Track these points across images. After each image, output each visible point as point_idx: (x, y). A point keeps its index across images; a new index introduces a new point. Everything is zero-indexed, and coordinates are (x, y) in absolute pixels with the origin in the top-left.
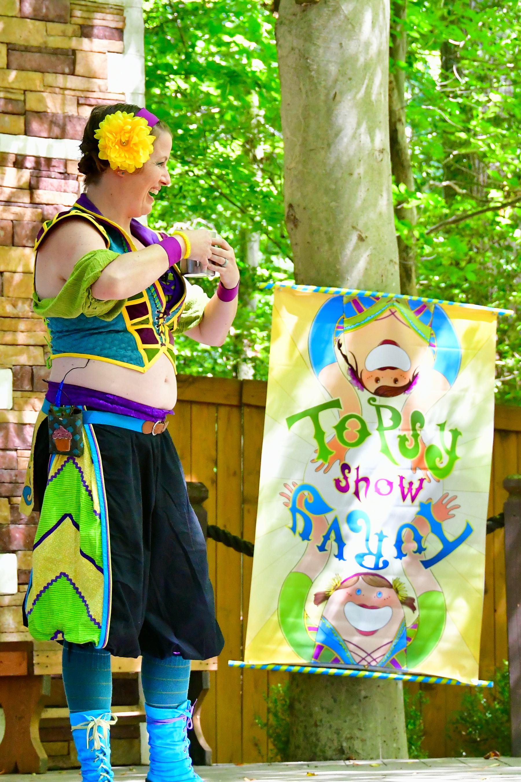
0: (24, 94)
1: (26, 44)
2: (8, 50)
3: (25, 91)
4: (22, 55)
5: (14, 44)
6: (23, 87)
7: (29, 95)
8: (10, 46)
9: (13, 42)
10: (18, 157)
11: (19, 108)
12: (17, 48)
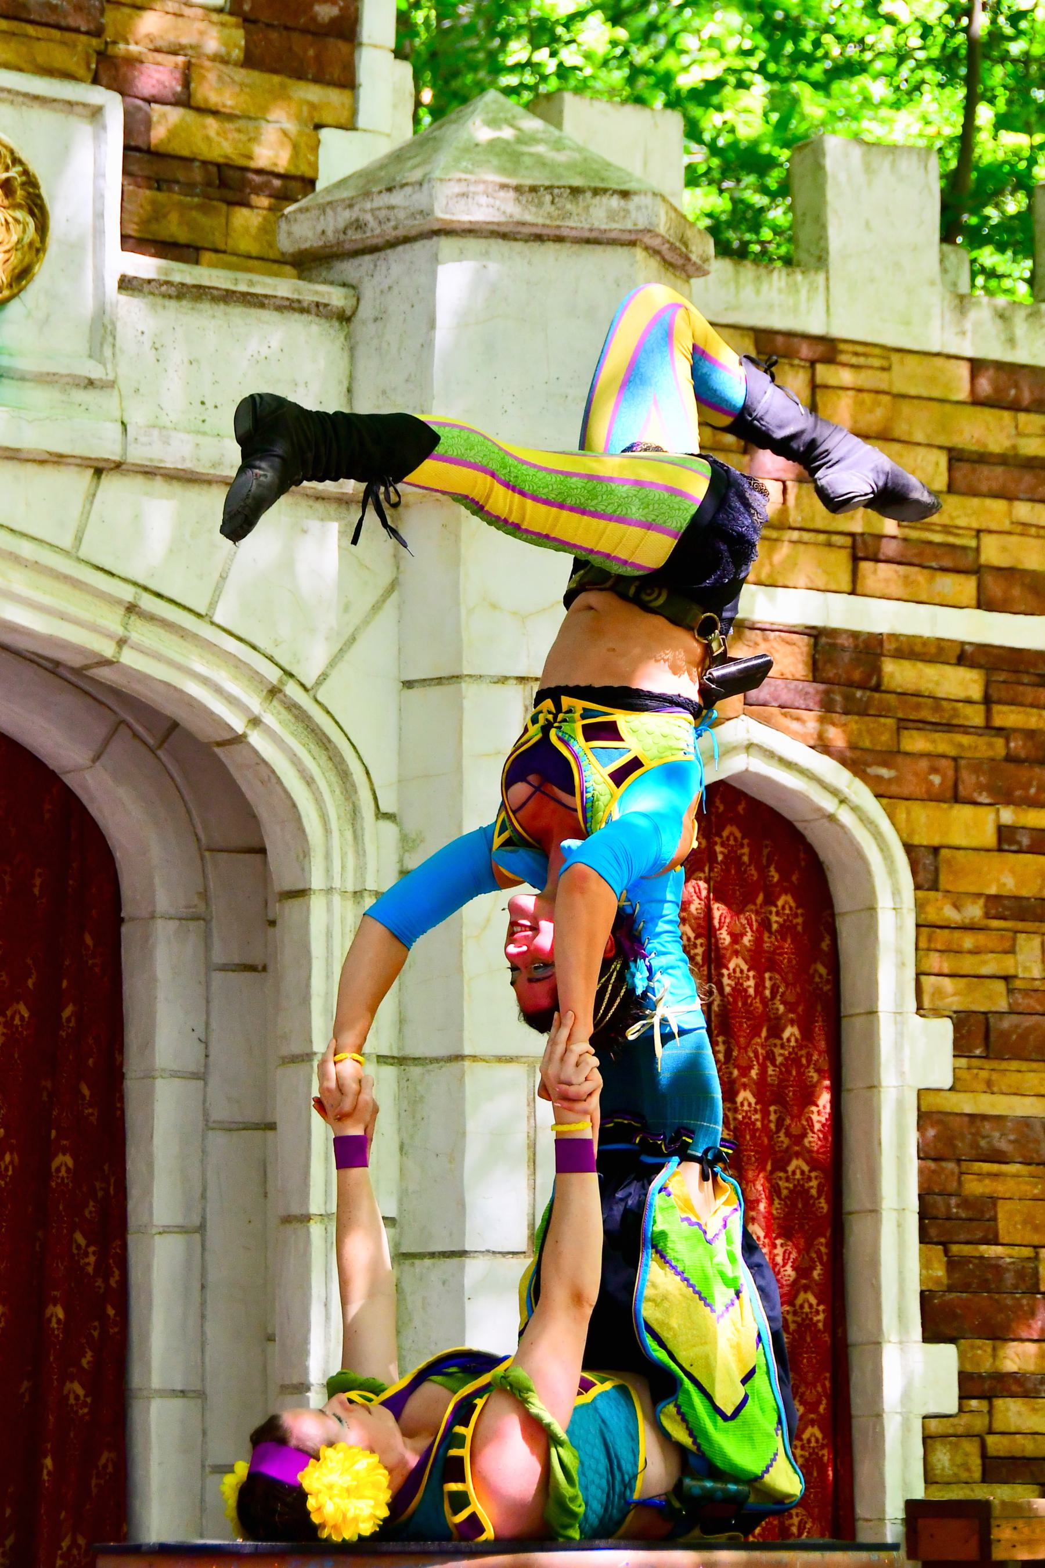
1: (982, 450)
2: (950, 461)
3: (979, 531)
4: (974, 471)
5: (962, 451)
6: (975, 525)
8: (954, 454)
9: (960, 446)
10: (967, 647)
11: (967, 562)
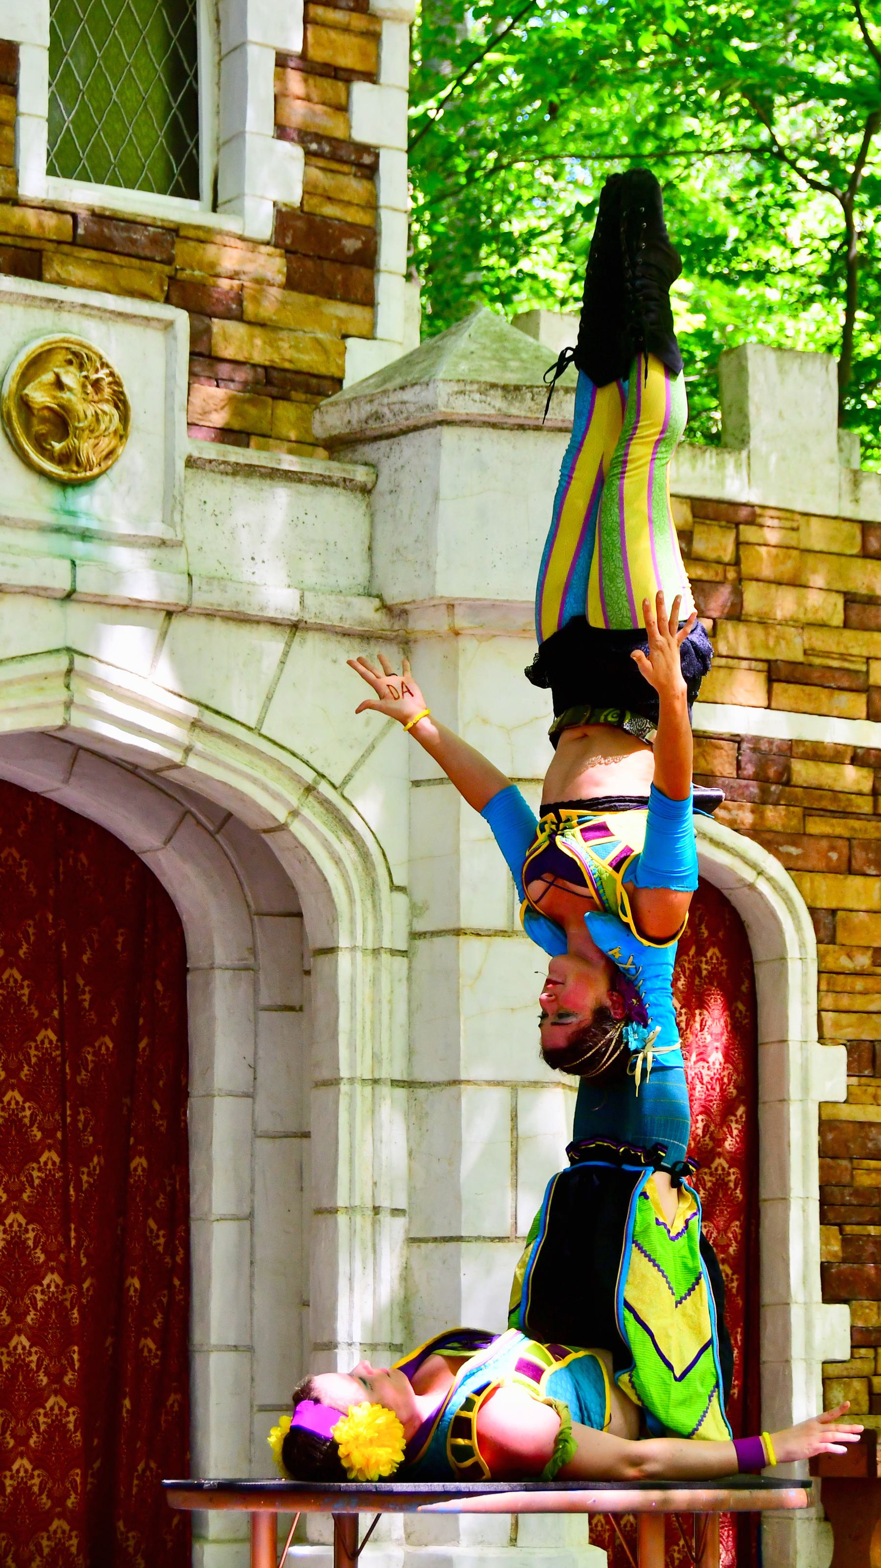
0: (867, 663)
1: (870, 593)
2: (846, 602)
3: (868, 659)
4: (864, 610)
5: (855, 594)
6: (865, 654)
7: (874, 665)
8: (849, 597)
9: (853, 591)
10: (859, 751)
11: (859, 682)
12: (858, 598)
